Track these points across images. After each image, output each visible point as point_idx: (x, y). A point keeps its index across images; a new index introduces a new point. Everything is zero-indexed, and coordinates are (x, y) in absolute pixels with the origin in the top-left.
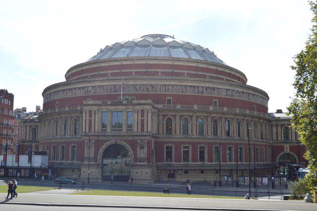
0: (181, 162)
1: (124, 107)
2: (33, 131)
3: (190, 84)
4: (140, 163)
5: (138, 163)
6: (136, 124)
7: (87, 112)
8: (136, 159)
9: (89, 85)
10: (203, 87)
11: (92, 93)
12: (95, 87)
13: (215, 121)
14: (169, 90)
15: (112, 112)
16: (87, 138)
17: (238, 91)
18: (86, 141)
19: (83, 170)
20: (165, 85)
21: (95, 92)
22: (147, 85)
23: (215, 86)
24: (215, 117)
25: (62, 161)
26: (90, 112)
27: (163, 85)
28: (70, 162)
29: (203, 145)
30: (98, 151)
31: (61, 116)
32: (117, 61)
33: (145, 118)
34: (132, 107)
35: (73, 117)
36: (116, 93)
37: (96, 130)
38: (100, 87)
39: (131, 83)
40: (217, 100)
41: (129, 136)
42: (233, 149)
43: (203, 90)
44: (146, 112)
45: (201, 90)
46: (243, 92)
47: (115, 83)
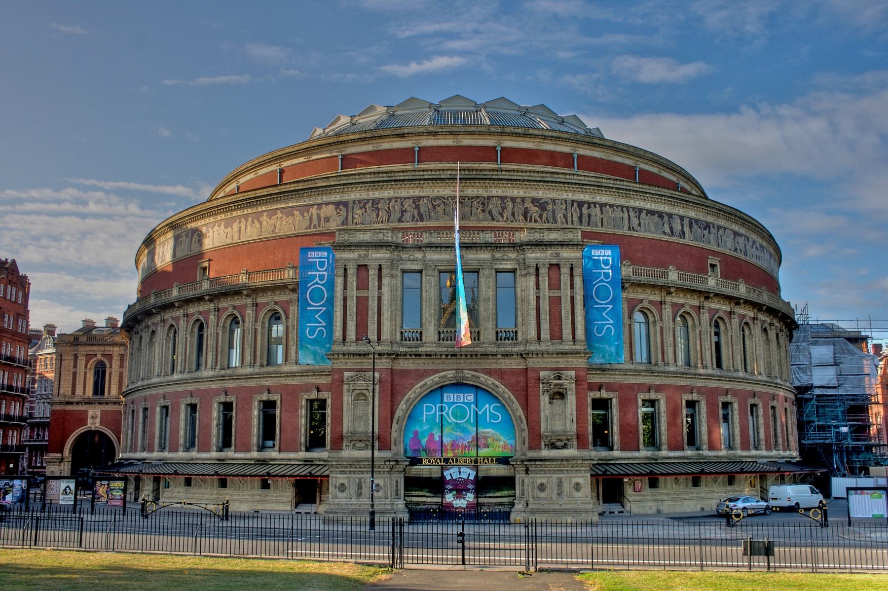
0: (638, 449)
1: (485, 255)
2: (97, 373)
3: (649, 206)
4: (554, 453)
5: (545, 453)
6: (533, 313)
7: (351, 271)
8: (535, 439)
9: (325, 199)
10: (682, 218)
11: (333, 226)
12: (345, 204)
13: (717, 326)
14: (592, 219)
15: (440, 272)
16: (351, 363)
17: (754, 242)
18: (346, 374)
19: (337, 478)
20: (581, 204)
21: (343, 224)
22: (523, 200)
23: (710, 219)
24: (717, 310)
25: (222, 455)
26: (362, 268)
27: (573, 202)
28: (255, 454)
29: (695, 397)
30: (393, 413)
31: (221, 306)
32: (402, 136)
33: (565, 292)
34: (513, 255)
35: (268, 304)
36: (420, 224)
37: (385, 335)
38: (362, 204)
39: (471, 192)
40: (715, 261)
41: (507, 355)
42: (761, 411)
43: (682, 225)
44: (565, 271)
45: (677, 227)
46: (761, 246)
47: (417, 192)
